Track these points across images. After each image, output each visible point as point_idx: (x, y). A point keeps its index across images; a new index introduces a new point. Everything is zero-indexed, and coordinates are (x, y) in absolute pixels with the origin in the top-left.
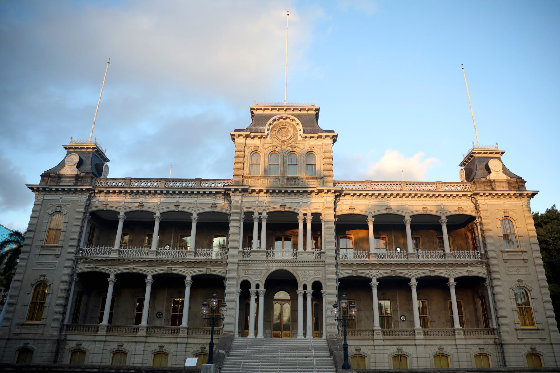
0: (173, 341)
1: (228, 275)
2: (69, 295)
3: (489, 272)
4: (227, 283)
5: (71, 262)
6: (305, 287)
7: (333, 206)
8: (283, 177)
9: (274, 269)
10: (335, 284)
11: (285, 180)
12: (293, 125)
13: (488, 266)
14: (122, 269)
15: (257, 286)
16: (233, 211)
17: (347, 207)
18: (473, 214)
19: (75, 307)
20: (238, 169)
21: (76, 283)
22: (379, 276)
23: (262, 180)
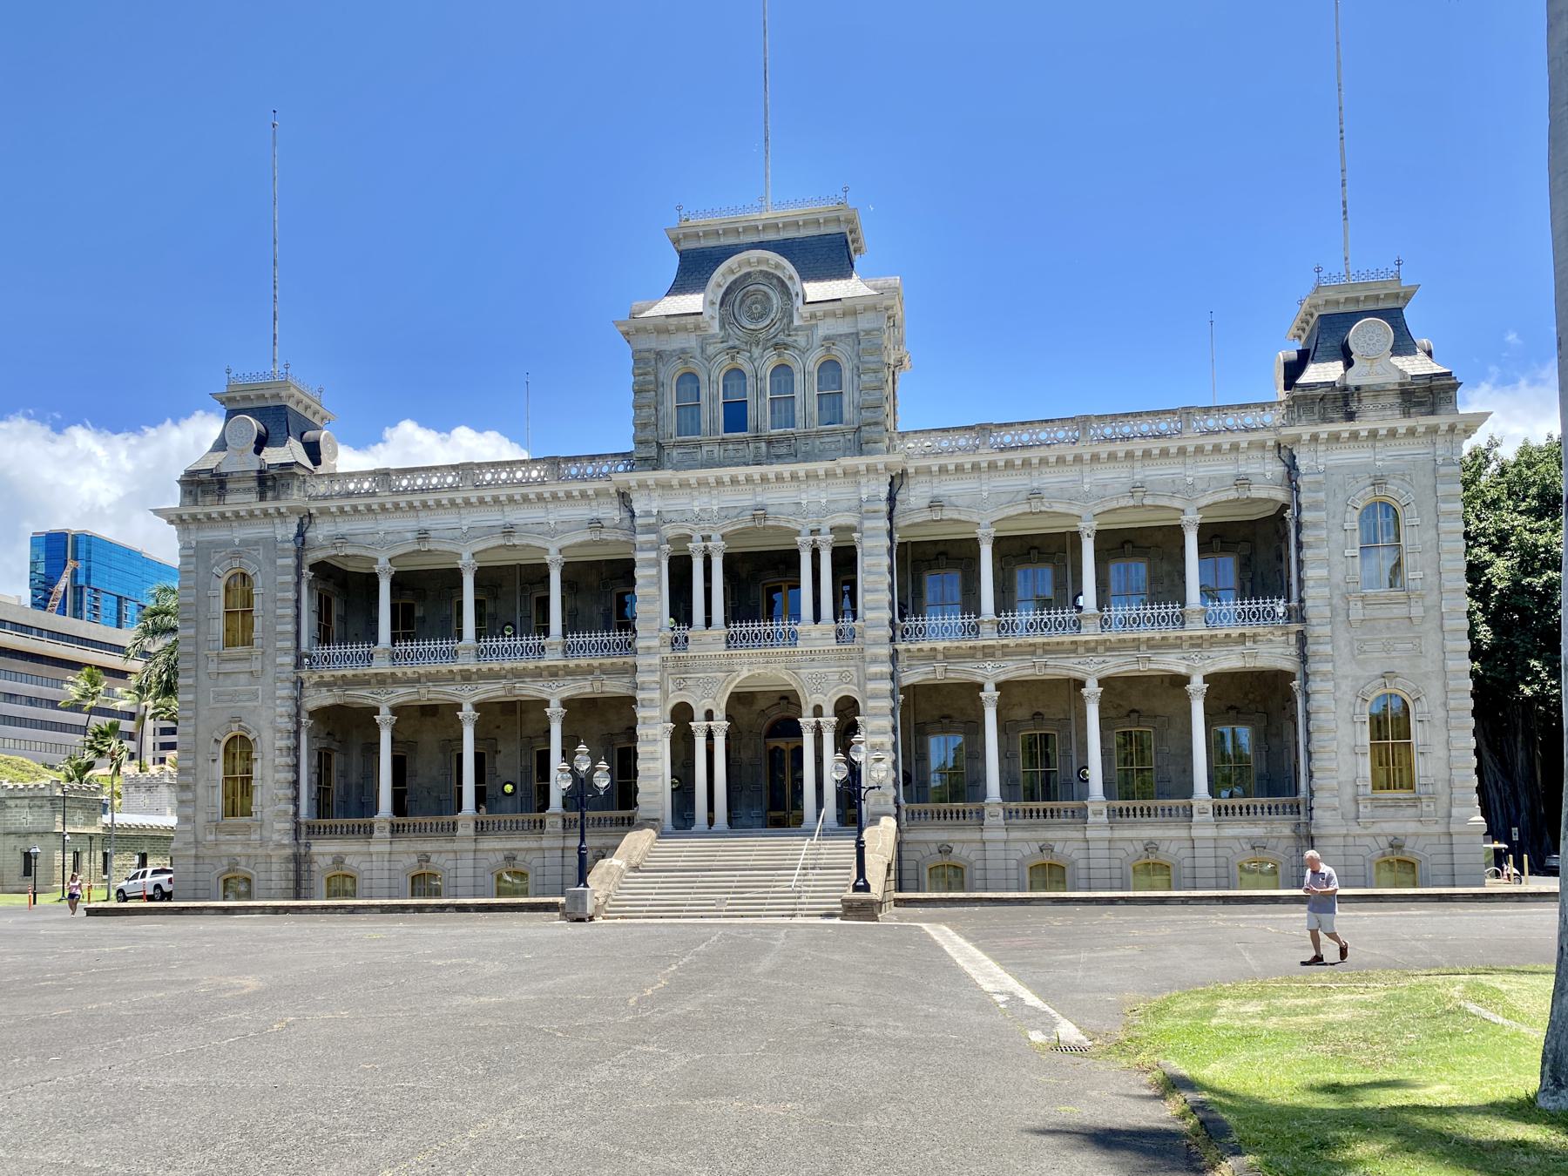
0: (534, 845)
1: (640, 695)
2: (298, 758)
3: (1304, 658)
4: (641, 713)
5: (289, 685)
6: (818, 711)
7: (884, 507)
8: (757, 438)
9: (745, 673)
10: (887, 704)
11: (763, 445)
12: (779, 278)
13: (1302, 639)
14: (402, 695)
15: (709, 715)
16: (640, 538)
17: (926, 502)
18: (1281, 495)
19: (319, 782)
20: (645, 425)
21: (310, 730)
22: (1002, 678)
23: (705, 449)
